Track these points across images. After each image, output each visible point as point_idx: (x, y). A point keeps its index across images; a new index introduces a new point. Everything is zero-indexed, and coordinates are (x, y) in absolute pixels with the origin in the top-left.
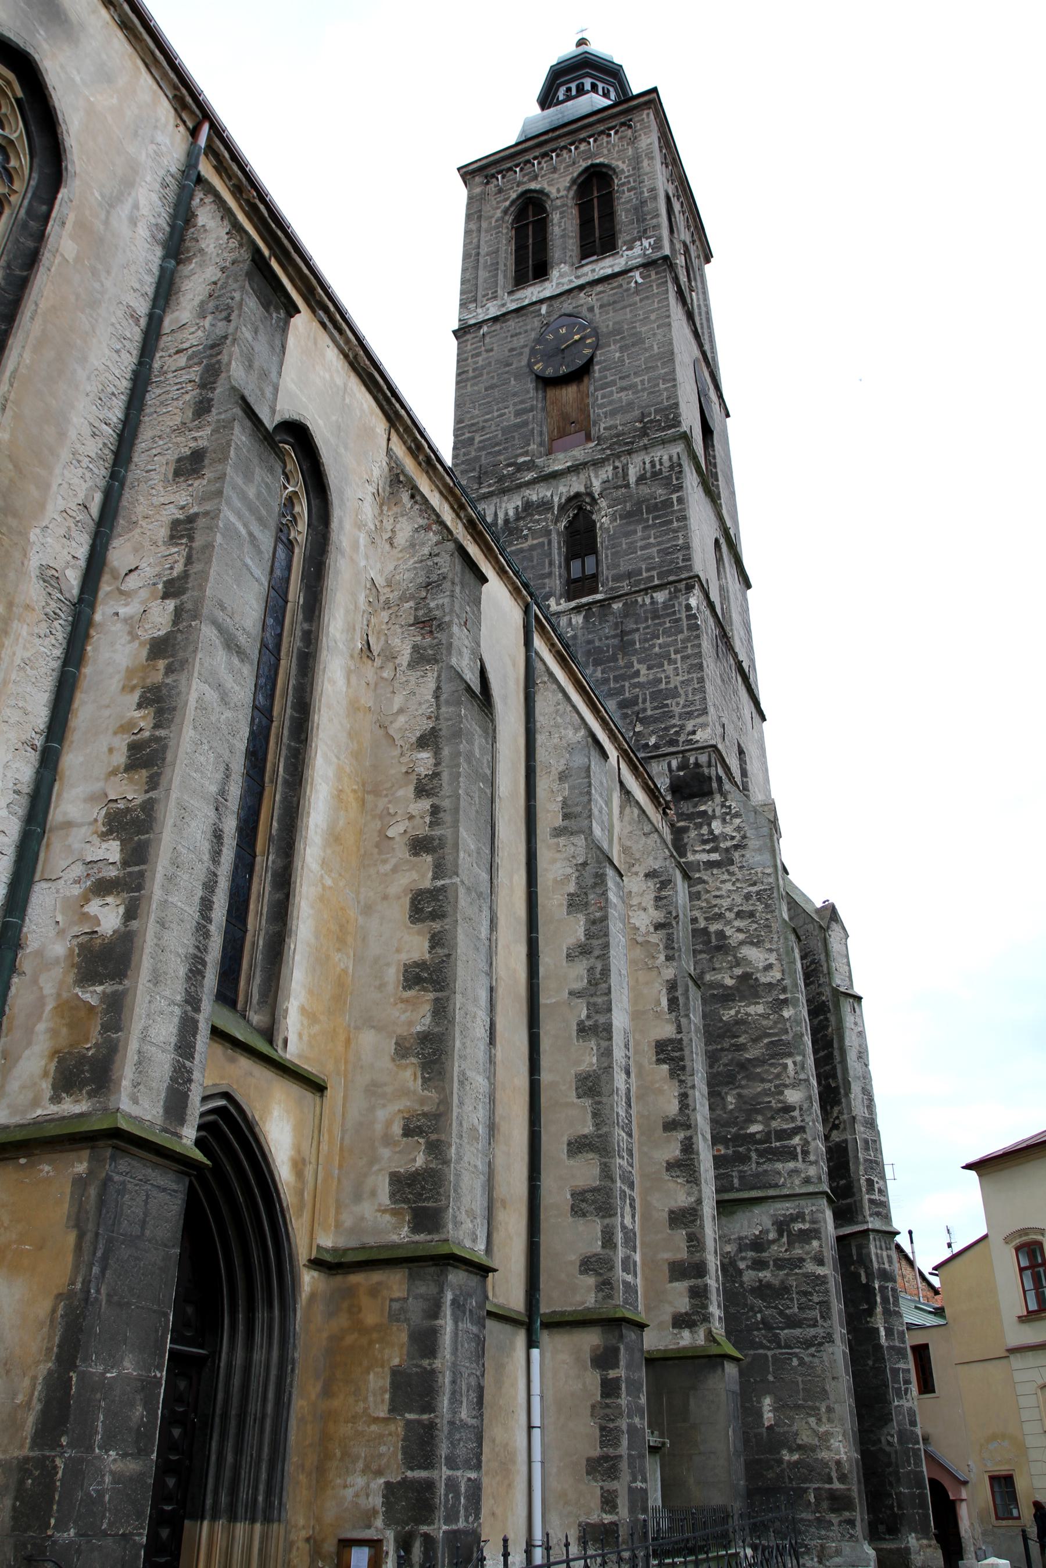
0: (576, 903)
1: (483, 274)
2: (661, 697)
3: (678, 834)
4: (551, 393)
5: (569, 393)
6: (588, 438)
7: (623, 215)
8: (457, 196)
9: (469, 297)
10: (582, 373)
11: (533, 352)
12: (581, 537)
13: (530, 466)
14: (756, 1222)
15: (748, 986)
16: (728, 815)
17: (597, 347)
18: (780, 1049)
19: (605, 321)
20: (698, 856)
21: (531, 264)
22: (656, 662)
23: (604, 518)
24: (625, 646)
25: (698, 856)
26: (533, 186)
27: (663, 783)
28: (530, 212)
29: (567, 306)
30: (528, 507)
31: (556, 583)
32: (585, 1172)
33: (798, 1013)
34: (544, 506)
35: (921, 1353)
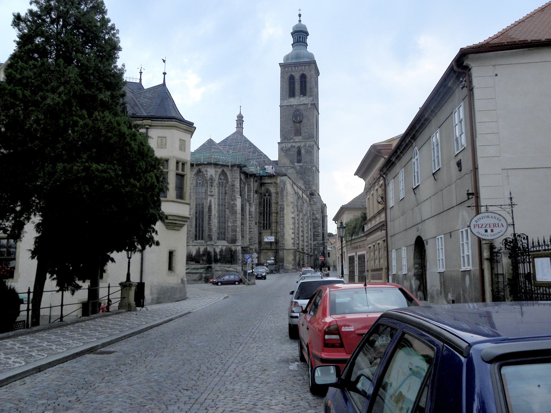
0: (306, 222)
1: (284, 93)
2: (309, 181)
3: (310, 200)
4: (296, 124)
5: (298, 124)
6: (301, 135)
7: (308, 90)
8: (279, 69)
9: (282, 99)
10: (300, 122)
11: (293, 116)
12: (299, 153)
13: (292, 139)
14: (315, 243)
15: (316, 219)
16: (316, 198)
17: (303, 118)
18: (319, 226)
19: (305, 113)
20: (312, 203)
21: (292, 94)
22: (309, 176)
23: (303, 151)
24: (305, 173)
25: (312, 203)
26: (293, 74)
27: (308, 194)
28: (292, 79)
29: (298, 108)
30: (292, 146)
31: (296, 160)
32: (307, 244)
33: (321, 222)
34: (294, 147)
35: (329, 253)
